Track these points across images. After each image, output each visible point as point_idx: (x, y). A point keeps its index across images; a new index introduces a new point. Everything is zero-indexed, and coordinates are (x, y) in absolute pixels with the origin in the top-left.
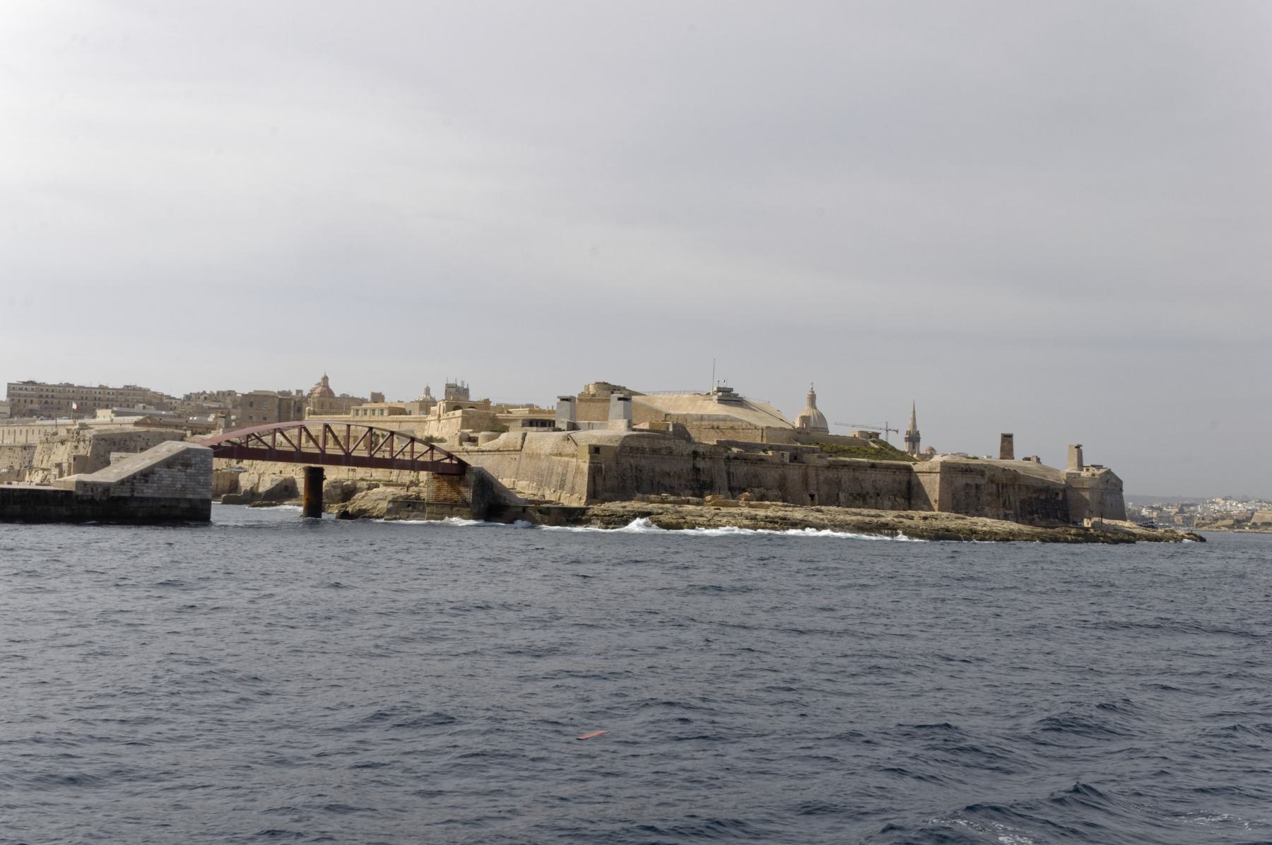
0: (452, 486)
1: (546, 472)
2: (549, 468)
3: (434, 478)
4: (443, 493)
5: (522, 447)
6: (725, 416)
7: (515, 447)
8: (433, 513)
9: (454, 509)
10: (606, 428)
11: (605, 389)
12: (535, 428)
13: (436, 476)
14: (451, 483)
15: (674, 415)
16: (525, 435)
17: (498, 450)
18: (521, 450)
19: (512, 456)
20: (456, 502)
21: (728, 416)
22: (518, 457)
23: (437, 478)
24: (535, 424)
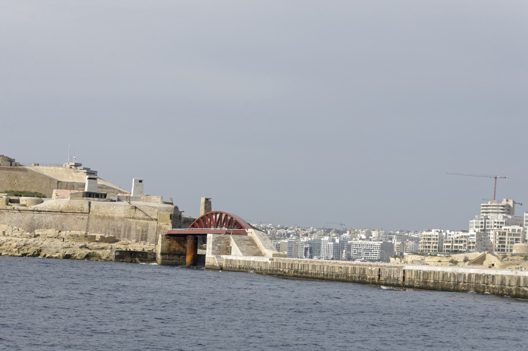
0: (179, 243)
1: (122, 229)
2: (126, 226)
3: (167, 238)
4: (173, 247)
5: (89, 211)
6: (102, 185)
7: (81, 210)
8: (166, 259)
9: (181, 257)
10: (139, 201)
11: (6, 161)
12: (96, 199)
13: (168, 237)
14: (179, 242)
15: (64, 182)
16: (90, 203)
17: (61, 212)
18: (89, 213)
19: (78, 216)
20: (182, 253)
21: (104, 185)
22: (86, 217)
23: (169, 238)
24: (92, 196)
